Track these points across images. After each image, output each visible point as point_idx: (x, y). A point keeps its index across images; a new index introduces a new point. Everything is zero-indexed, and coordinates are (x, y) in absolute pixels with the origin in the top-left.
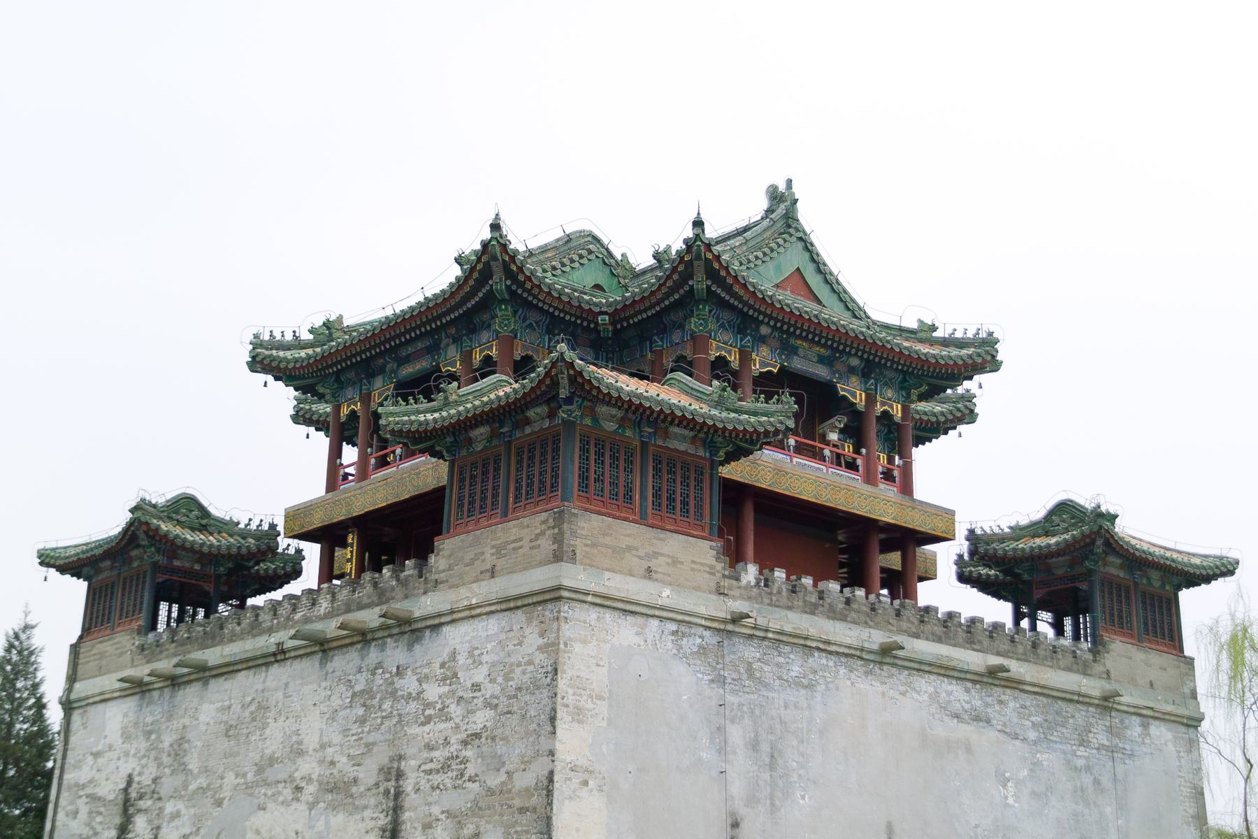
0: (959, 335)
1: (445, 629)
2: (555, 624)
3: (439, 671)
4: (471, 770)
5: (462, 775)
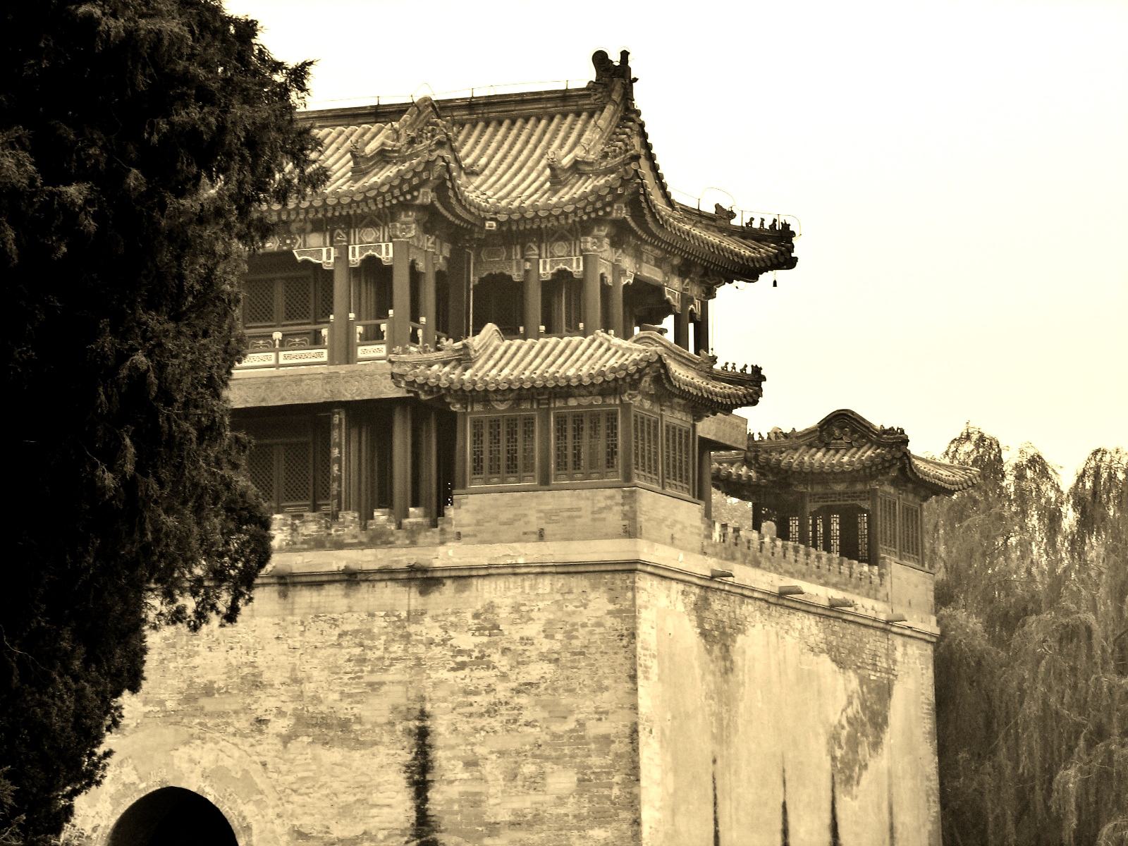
0: (756, 225)
1: (474, 581)
2: (630, 594)
3: (471, 621)
4: (527, 716)
5: (515, 721)
